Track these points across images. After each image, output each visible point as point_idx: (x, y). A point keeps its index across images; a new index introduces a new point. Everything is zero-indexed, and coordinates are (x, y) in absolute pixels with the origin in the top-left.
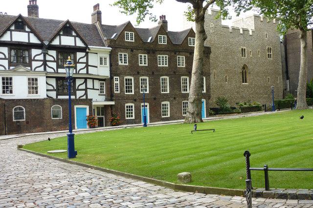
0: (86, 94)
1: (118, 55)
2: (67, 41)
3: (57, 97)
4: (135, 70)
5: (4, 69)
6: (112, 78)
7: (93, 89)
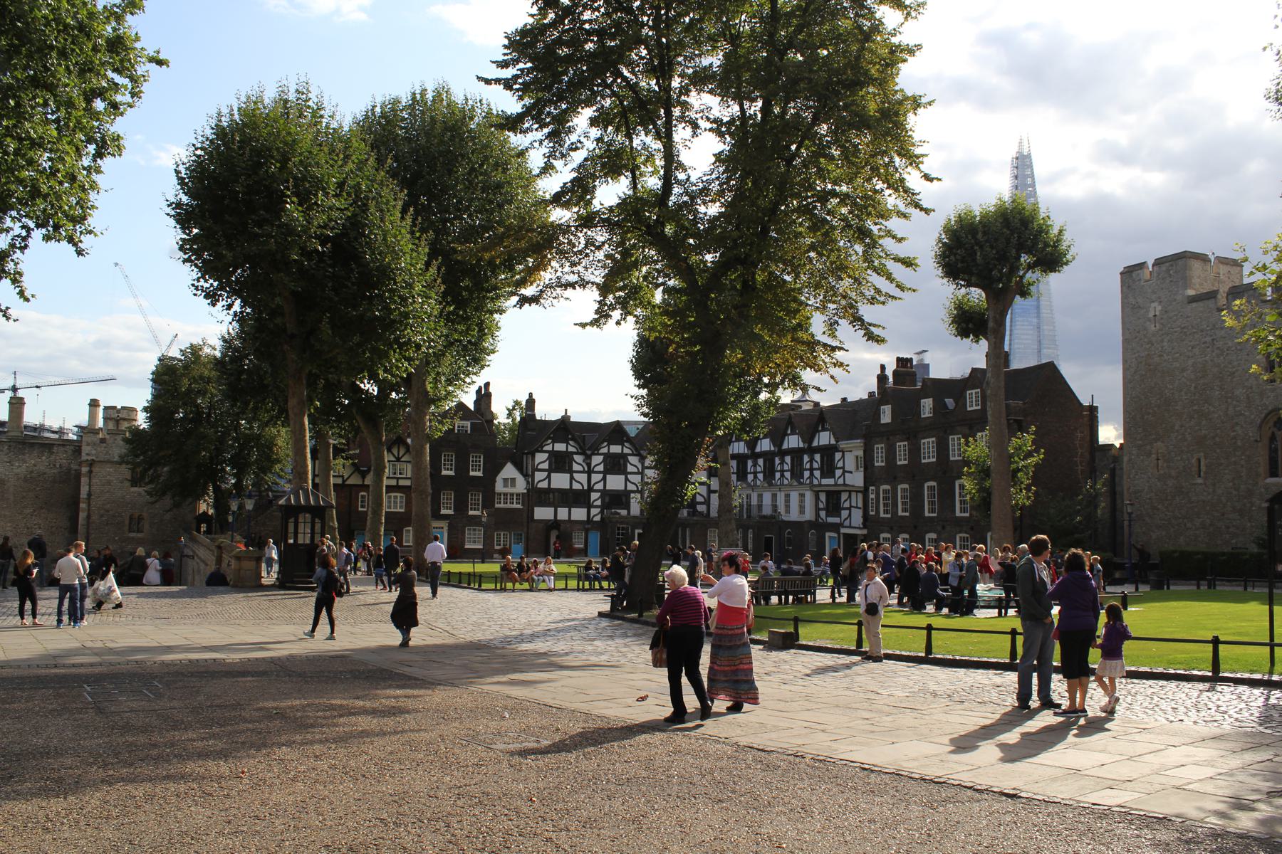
2: (824, 438)
4: (892, 474)
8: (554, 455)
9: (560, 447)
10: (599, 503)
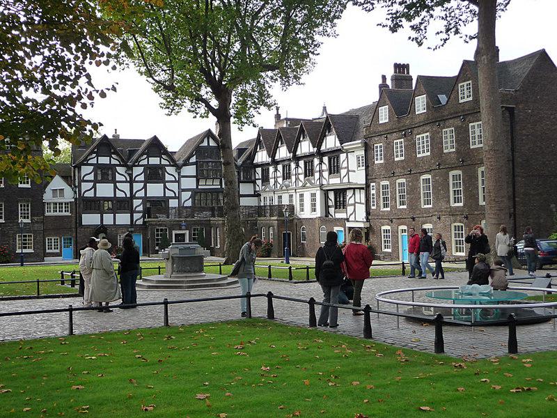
4: (391, 170)
7: (360, 203)
8: (98, 167)
9: (104, 160)
10: (141, 208)
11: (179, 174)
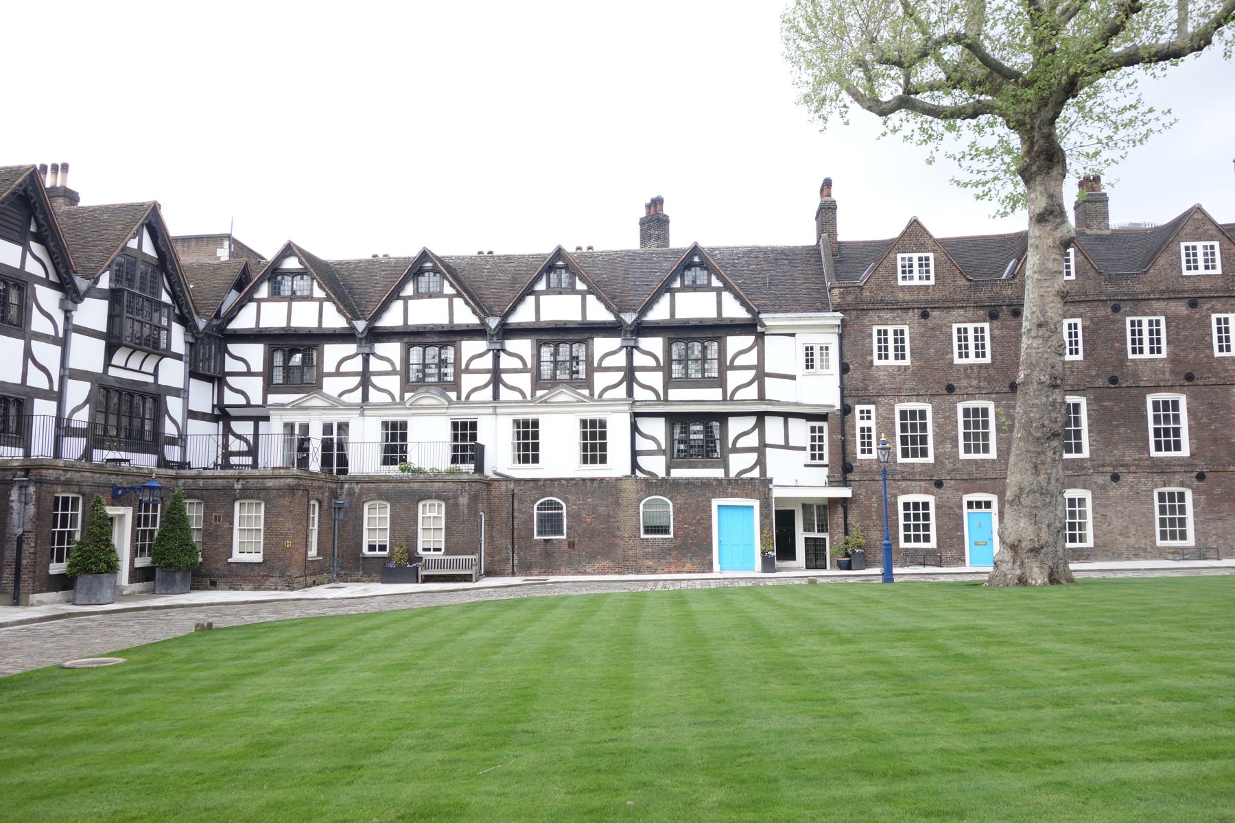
0: (761, 463)
1: (870, 336)
3: (668, 473)
5: (519, 397)
6: (846, 410)
7: (787, 446)
11: (67, 319)
